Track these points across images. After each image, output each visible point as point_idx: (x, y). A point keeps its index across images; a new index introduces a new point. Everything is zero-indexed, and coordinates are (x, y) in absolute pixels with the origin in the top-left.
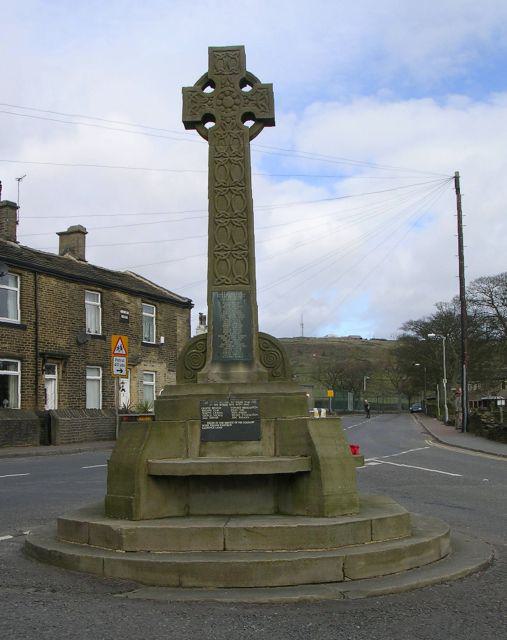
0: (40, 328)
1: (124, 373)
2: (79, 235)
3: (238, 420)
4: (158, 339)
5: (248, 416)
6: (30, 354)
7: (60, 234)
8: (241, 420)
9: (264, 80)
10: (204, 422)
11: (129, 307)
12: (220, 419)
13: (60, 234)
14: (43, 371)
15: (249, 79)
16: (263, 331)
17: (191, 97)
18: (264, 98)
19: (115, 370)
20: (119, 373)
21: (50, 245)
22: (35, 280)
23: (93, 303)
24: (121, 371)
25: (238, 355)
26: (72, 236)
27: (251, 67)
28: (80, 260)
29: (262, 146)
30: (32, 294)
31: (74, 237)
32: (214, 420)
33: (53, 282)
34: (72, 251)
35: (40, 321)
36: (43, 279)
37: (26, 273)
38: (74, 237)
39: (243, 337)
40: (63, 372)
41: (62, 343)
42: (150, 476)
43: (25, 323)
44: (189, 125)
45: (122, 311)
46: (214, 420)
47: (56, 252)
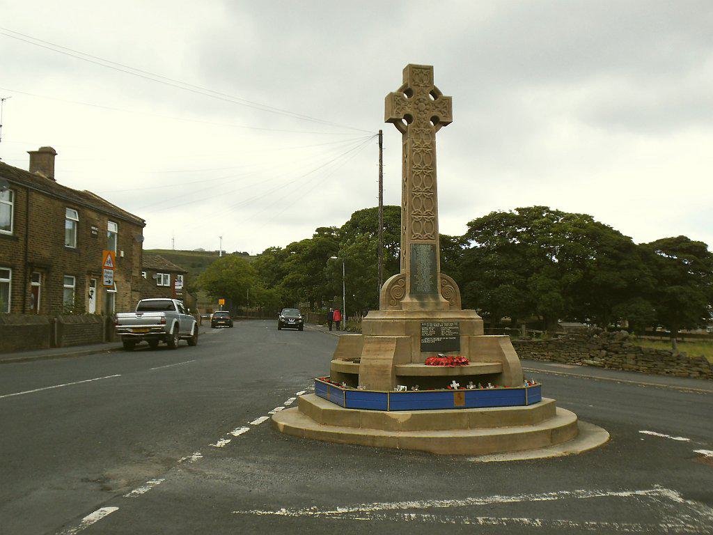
0: (29, 240)
1: (111, 284)
2: (48, 155)
3: (446, 336)
4: (119, 252)
5: (452, 334)
6: (20, 264)
7: (31, 153)
8: (448, 337)
9: (445, 93)
10: (423, 338)
11: (98, 224)
12: (434, 336)
13: (31, 153)
14: (30, 278)
15: (436, 93)
16: (165, 245)
17: (393, 101)
18: (446, 107)
19: (104, 281)
20: (107, 284)
21: (24, 164)
22: (28, 196)
23: (72, 216)
24: (110, 282)
25: (427, 289)
26: (44, 155)
27: (438, 83)
28: (50, 178)
29: (443, 138)
30: (24, 208)
31: (44, 158)
32: (430, 337)
33: (42, 199)
34: (44, 170)
35: (30, 233)
36: (35, 195)
37: (20, 190)
38: (44, 158)
39: (430, 276)
40: (46, 280)
41: (46, 254)
42: (397, 376)
43: (17, 235)
44: (389, 121)
45: (92, 228)
46: (430, 337)
47: (28, 170)
